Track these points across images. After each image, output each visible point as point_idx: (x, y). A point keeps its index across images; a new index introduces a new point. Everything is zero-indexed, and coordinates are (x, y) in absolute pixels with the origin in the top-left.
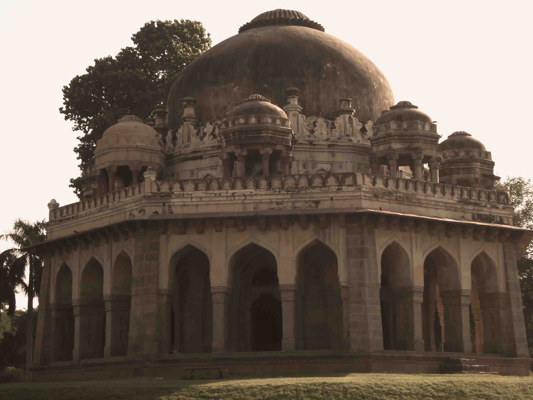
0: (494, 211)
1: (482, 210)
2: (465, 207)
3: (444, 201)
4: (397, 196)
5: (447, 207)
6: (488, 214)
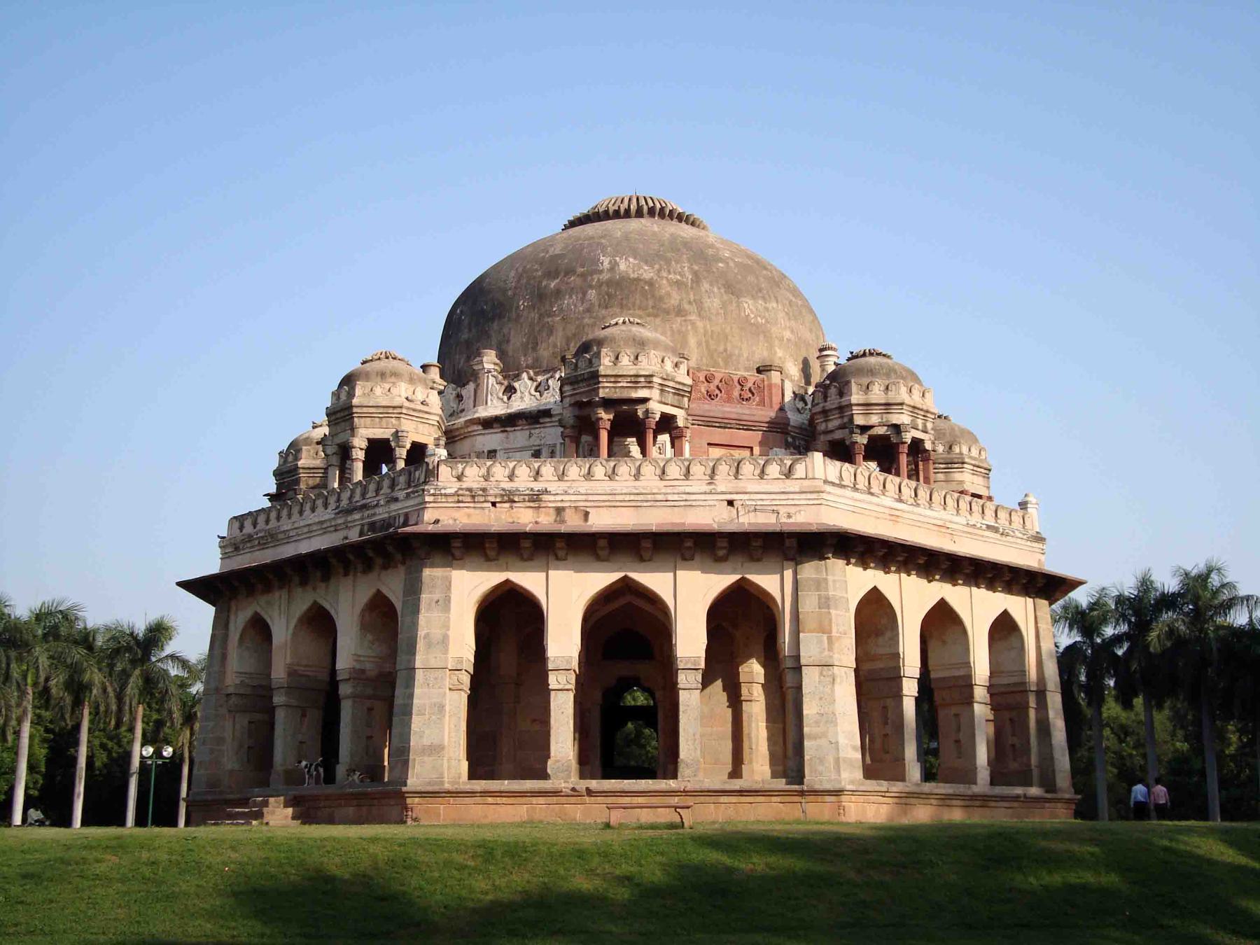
0: (394, 506)
1: (374, 515)
2: (349, 519)
3: (317, 520)
4: (258, 538)
5: (324, 528)
6: (386, 515)
